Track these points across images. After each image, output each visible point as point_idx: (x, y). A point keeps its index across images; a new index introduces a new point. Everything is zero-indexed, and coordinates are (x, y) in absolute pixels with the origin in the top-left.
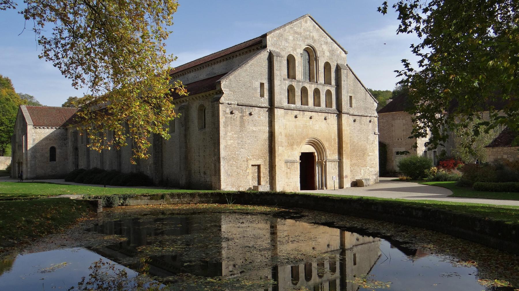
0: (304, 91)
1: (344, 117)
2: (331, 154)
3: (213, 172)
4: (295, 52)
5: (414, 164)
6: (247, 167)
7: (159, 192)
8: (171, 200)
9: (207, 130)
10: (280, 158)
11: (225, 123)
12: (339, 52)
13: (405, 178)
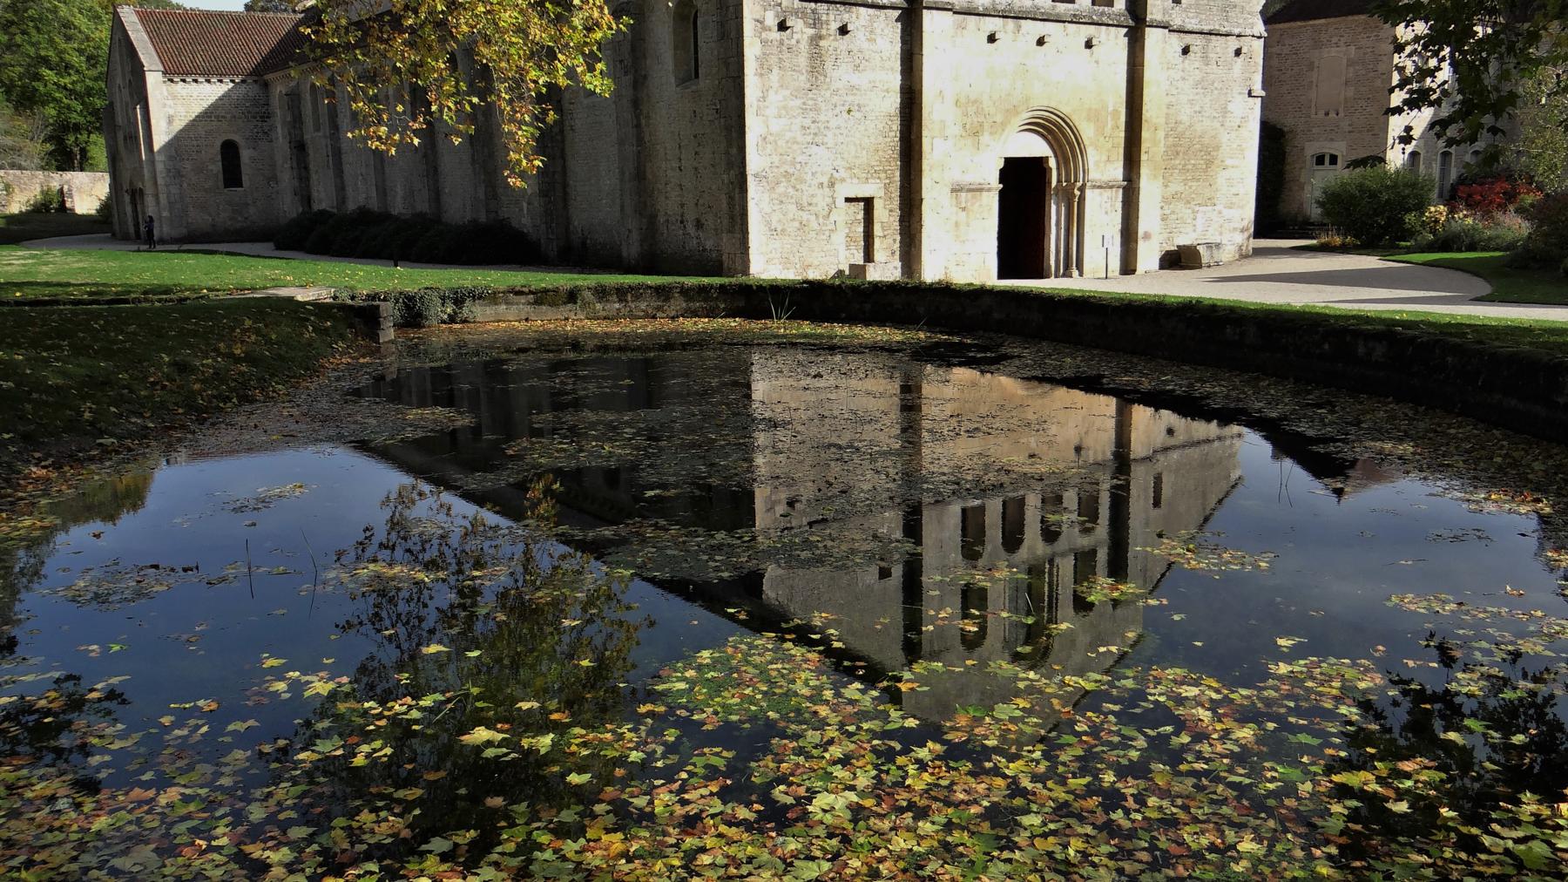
1: (1153, 39)
2: (1102, 163)
3: (725, 222)
5: (1373, 195)
6: (832, 207)
7: (562, 282)
8: (599, 306)
9: (705, 83)
11: (762, 61)
13: (1338, 240)
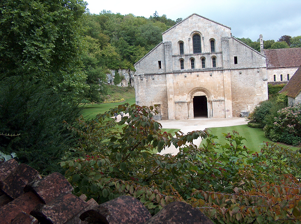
0: (192, 60)
4: (184, 39)
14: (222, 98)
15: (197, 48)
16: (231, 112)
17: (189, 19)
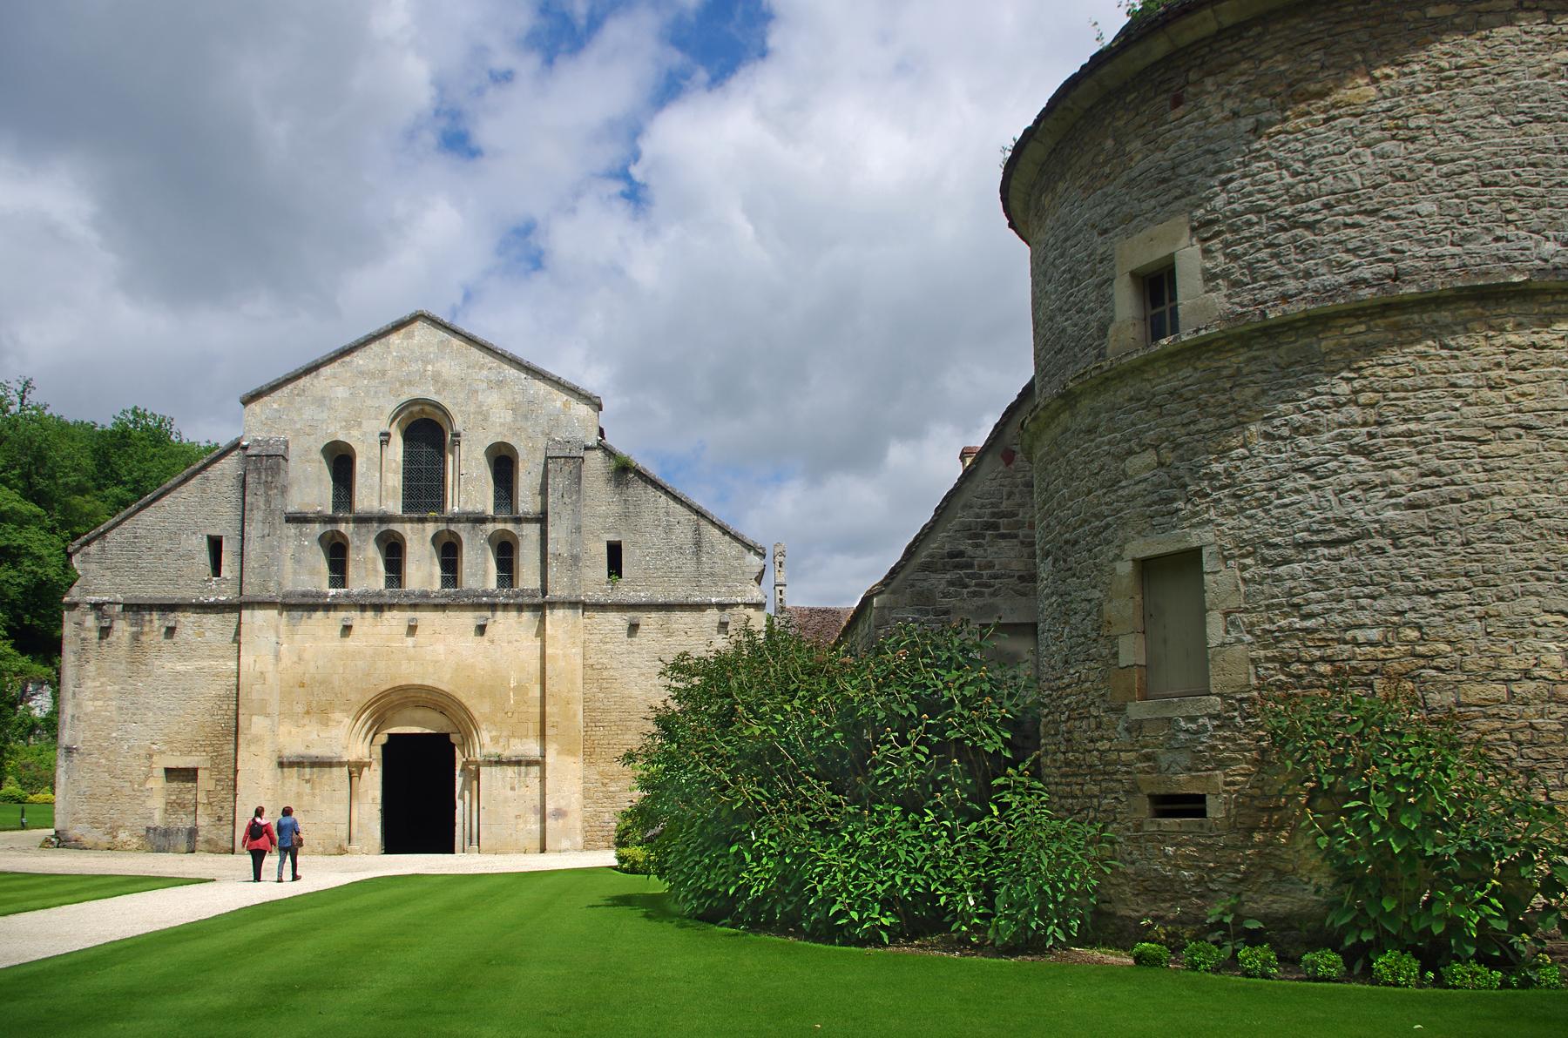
4: (355, 433)
10: (253, 748)
12: (559, 404)
14: (532, 749)
15: (424, 488)
16: (575, 821)
17: (395, 339)
